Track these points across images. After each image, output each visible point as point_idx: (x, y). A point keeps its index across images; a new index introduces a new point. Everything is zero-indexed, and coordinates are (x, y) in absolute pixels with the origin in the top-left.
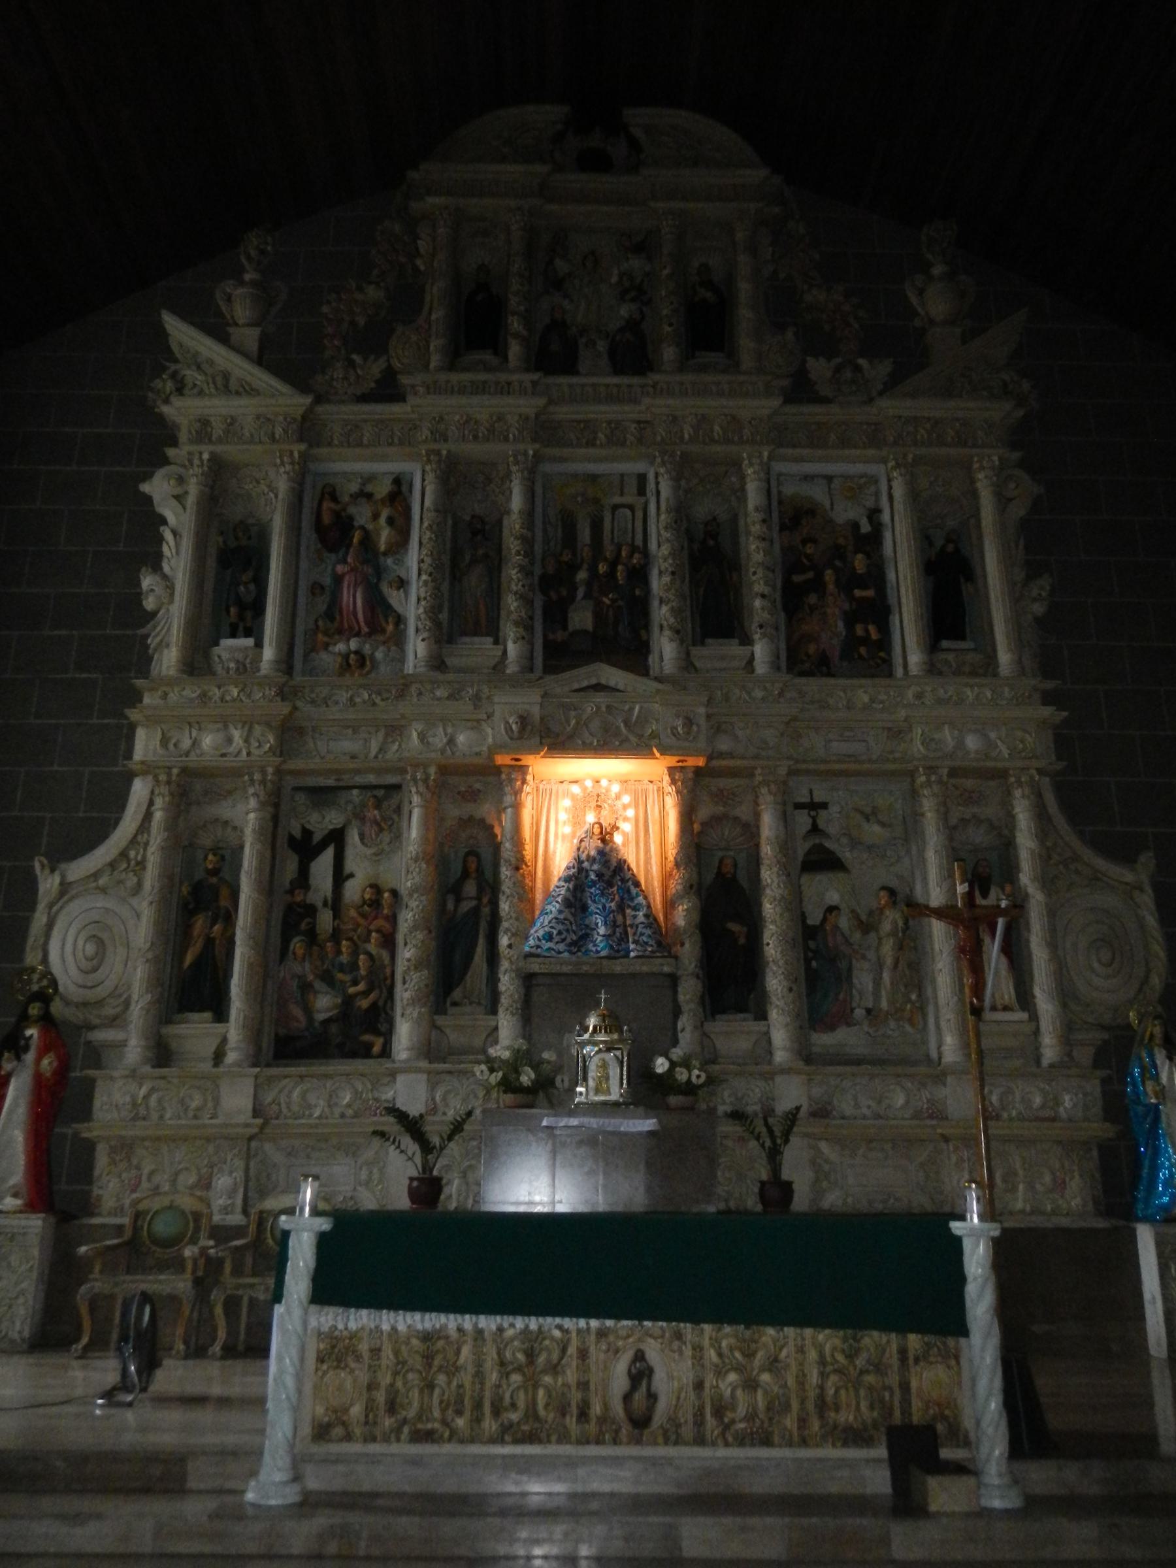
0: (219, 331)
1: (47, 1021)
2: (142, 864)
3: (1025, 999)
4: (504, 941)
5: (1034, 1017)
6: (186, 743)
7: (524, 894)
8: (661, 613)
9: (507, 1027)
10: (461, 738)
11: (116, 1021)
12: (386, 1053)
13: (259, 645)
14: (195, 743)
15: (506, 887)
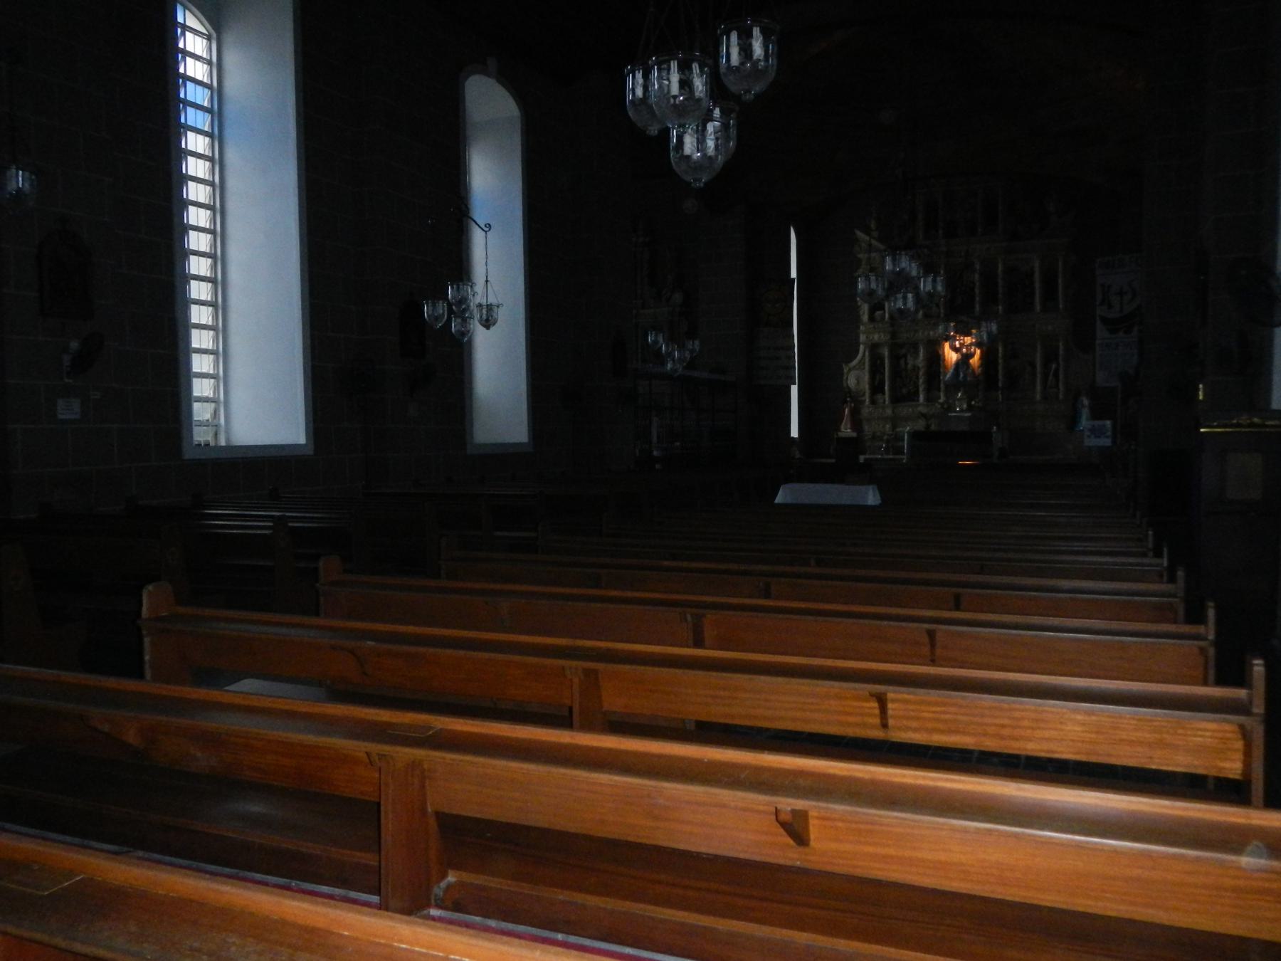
0: (867, 231)
1: (850, 397)
2: (864, 363)
3: (1057, 386)
4: (941, 378)
5: (1059, 389)
6: (871, 338)
7: (946, 367)
8: (977, 299)
9: (942, 395)
10: (931, 333)
11: (864, 395)
12: (918, 401)
13: (885, 312)
14: (873, 338)
15: (942, 365)
